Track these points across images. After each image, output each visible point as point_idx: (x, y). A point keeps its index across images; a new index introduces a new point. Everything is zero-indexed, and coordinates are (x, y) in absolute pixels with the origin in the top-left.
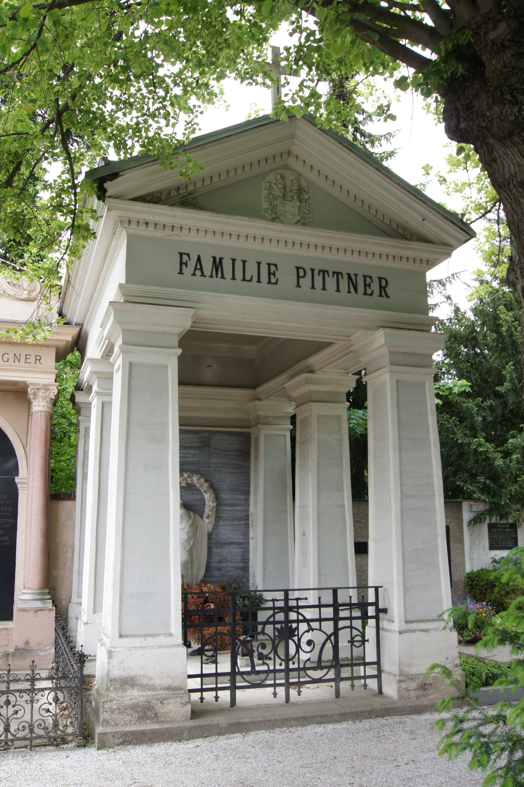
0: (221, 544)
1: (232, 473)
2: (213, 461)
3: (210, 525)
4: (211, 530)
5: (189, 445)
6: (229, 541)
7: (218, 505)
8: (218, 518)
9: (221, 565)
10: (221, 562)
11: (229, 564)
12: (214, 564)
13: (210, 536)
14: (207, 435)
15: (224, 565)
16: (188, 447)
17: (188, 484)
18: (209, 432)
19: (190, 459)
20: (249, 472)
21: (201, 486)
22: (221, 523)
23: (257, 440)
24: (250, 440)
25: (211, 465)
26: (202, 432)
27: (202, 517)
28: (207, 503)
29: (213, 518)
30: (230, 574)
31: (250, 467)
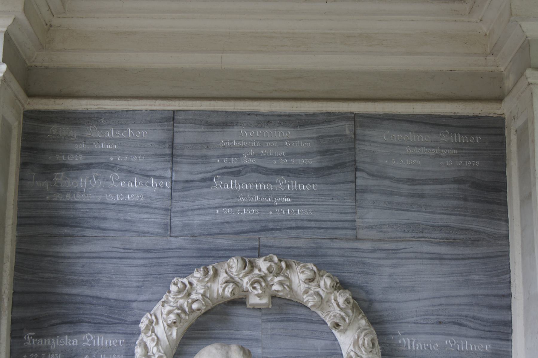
1: (441, 258)
2: (371, 216)
5: (283, 163)
14: (347, 128)
16: (279, 172)
17: (274, 297)
18: (354, 117)
20: (506, 255)
21: (322, 302)
23: (525, 135)
24: (503, 144)
25: (362, 233)
26: (329, 118)
31: (507, 237)
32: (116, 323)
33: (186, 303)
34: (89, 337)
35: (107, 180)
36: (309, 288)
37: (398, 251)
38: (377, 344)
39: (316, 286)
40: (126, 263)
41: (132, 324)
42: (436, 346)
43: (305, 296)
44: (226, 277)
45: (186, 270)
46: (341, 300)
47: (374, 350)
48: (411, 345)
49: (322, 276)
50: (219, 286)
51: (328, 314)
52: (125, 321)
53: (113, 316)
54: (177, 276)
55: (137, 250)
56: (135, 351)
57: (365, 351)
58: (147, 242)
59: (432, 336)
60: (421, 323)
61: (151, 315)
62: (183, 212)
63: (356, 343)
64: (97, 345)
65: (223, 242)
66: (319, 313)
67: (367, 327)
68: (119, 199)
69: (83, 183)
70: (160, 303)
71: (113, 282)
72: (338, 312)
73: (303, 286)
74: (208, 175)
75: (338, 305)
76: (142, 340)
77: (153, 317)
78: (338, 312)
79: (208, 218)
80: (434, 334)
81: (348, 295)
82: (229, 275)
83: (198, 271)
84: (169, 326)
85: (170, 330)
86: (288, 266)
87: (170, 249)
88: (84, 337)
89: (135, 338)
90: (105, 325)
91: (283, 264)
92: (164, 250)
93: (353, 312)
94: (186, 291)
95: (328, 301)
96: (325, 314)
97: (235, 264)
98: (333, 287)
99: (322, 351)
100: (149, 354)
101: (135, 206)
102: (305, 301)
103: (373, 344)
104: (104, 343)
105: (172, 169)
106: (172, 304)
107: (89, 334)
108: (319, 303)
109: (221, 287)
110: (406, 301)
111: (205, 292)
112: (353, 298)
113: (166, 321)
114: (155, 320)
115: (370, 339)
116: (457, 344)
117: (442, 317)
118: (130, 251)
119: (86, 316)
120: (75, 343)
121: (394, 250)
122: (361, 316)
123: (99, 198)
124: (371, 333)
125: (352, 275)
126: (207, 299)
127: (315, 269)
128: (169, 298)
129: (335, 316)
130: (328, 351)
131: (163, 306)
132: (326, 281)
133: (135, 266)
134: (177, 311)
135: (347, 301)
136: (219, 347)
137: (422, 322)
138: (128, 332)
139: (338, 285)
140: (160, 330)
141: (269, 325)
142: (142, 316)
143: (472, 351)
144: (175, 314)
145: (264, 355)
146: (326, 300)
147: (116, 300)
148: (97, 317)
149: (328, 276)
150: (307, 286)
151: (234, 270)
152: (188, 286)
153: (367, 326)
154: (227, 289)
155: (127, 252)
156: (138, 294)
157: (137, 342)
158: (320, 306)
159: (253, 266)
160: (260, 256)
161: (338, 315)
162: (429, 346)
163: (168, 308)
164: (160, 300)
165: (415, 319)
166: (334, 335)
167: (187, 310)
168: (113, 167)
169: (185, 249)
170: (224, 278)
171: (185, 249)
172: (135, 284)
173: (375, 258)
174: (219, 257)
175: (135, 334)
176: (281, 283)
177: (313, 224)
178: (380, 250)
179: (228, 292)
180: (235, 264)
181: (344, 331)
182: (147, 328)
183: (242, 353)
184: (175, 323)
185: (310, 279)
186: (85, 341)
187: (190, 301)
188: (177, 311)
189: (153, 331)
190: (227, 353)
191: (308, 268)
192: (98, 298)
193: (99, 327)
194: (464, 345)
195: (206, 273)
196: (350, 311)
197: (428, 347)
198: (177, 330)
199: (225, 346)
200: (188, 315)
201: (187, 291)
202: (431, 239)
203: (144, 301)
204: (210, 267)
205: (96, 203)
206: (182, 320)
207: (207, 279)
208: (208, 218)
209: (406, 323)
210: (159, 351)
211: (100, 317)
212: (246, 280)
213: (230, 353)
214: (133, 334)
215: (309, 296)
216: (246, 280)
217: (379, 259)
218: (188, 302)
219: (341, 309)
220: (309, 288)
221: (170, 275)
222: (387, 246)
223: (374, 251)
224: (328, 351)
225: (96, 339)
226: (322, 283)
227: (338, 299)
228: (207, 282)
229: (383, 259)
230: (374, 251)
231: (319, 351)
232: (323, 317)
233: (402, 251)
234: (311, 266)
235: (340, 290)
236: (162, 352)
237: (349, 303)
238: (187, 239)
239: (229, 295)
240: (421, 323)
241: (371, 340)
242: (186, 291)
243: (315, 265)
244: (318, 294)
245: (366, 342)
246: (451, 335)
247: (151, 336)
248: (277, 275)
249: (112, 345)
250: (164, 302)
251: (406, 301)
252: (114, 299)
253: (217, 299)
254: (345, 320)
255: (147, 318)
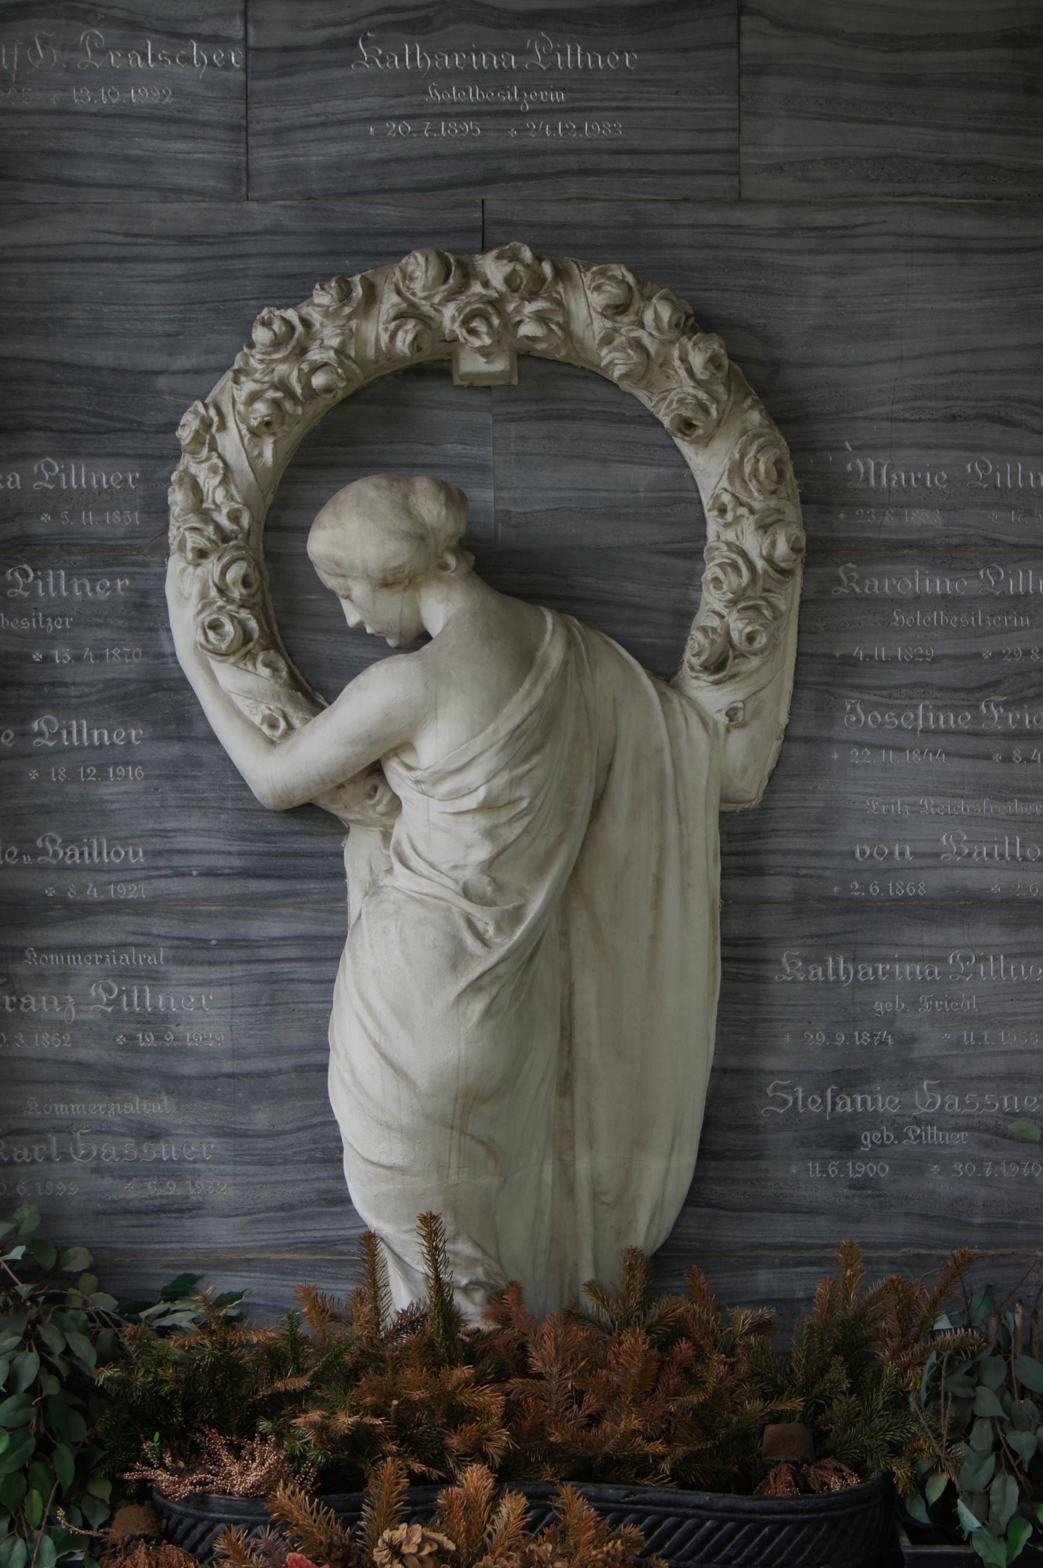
0: (855, 917)
1: (960, 248)
3: (737, 742)
4: (750, 788)
6: (927, 883)
7: (817, 552)
8: (822, 677)
9: (846, 1105)
10: (849, 1079)
11: (926, 1098)
12: (788, 1094)
13: (743, 839)
15: (882, 1101)
17: (524, 356)
19: (554, 132)
21: (649, 367)
22: (857, 716)
27: (664, 668)
28: (713, 527)
29: (771, 683)
30: (939, 1184)
32: (115, 431)
33: (295, 375)
34: (49, 468)
35: (74, 49)
36: (615, 330)
37: (848, 233)
38: (789, 473)
39: (632, 323)
40: (135, 273)
41: (157, 432)
42: (940, 478)
43: (604, 352)
44: (398, 304)
45: (296, 291)
46: (698, 360)
47: (782, 488)
48: (878, 476)
49: (650, 298)
50: (381, 326)
51: (665, 398)
52: (141, 424)
53: (107, 412)
54: (268, 306)
55: (162, 237)
56: (170, 499)
57: (759, 491)
58: (185, 215)
59: (933, 452)
60: (904, 420)
61: (206, 406)
62: (280, 134)
63: (735, 471)
64: (70, 487)
65: (387, 212)
66: (642, 395)
67: (766, 430)
68: (106, 99)
69: (10, 58)
70: (229, 374)
71: (105, 324)
72: (692, 391)
73: (600, 325)
74: (344, 31)
75: (690, 372)
76: (186, 471)
77: (212, 412)
78: (692, 391)
79: (347, 148)
80: (936, 446)
81: (716, 346)
82: (405, 299)
83: (323, 289)
84: (254, 433)
85: (256, 445)
86: (561, 274)
87: (247, 233)
88: (36, 468)
89: (168, 469)
90: (88, 436)
91: (547, 268)
92: (231, 237)
93: (729, 391)
94: (293, 342)
95: (666, 363)
96: (655, 399)
97: (419, 268)
98: (677, 325)
99: (650, 494)
100: (205, 505)
101: (152, 119)
102: (604, 363)
103: (781, 474)
104: (87, 482)
105: (245, 15)
106: (258, 376)
107: (48, 459)
108: (642, 369)
109: (386, 330)
110: (866, 363)
111: (343, 344)
112: (731, 357)
113: (244, 420)
114: (216, 419)
115: (772, 459)
116: (994, 471)
117: (959, 403)
118: (144, 241)
119: (37, 413)
120: (13, 483)
121: (839, 228)
122: (749, 402)
123: (54, 99)
124: (774, 444)
125: (727, 295)
126: (350, 363)
127: (630, 278)
128: (252, 361)
129: (681, 401)
130: (664, 494)
131: (236, 381)
132: (659, 308)
133: (159, 282)
134: (271, 394)
135: (713, 361)
136: (384, 483)
137: (907, 416)
138: (150, 452)
139: (691, 321)
140: (231, 443)
141: (513, 429)
142: (182, 410)
143: (1032, 489)
144: (267, 400)
145: (500, 507)
146: (660, 360)
147: (114, 371)
148: (68, 415)
149: (665, 298)
150: (609, 324)
151: (418, 286)
152: (300, 328)
153: (766, 426)
154: (400, 335)
155: (136, 244)
156: (171, 355)
157: (174, 477)
158: (643, 377)
159: (468, 274)
160: (484, 249)
161: (690, 400)
162: (924, 478)
163: (248, 386)
164: (228, 367)
165: (888, 408)
166: (679, 451)
167: (299, 391)
168: (88, 12)
169: (288, 233)
170: (393, 305)
171: (288, 233)
172: (160, 328)
173: (789, 252)
174: (379, 254)
175: (167, 457)
176: (541, 318)
177: (626, 162)
178: (802, 229)
179: (403, 342)
180: (419, 268)
181: (705, 442)
182: (198, 439)
183: (442, 497)
184: (268, 424)
185: (617, 307)
186: (40, 476)
187: (305, 367)
188: (271, 394)
189: (213, 448)
190: (406, 497)
191: (613, 278)
192: (65, 365)
193: (73, 440)
194: (1014, 474)
195: (345, 294)
196: (721, 389)
197: (921, 482)
198: (275, 443)
199: (398, 480)
200: (303, 404)
201: (298, 340)
202: (937, 199)
203: (185, 372)
204: (357, 278)
205: (46, 113)
206: (287, 418)
207: (347, 310)
208: (347, 148)
209: (866, 419)
210: (230, 497)
211: (73, 416)
212: (449, 310)
213: (412, 498)
214: (161, 457)
215: (616, 349)
216: (449, 310)
217: (800, 252)
218: (300, 370)
219: (699, 384)
220: (615, 330)
221: (252, 303)
222: (821, 218)
223: (786, 232)
224: (664, 494)
225: (67, 471)
226: (649, 317)
227: (691, 358)
228: (349, 317)
229: (811, 252)
230: (786, 232)
231: (642, 495)
232: (649, 405)
233: (860, 230)
234: (619, 271)
235: (695, 334)
236: (239, 500)
237: (718, 367)
238: (293, 207)
239: (406, 351)
240: (904, 420)
241: (775, 464)
242: (295, 343)
243: (630, 270)
244: (637, 345)
245: (762, 468)
246: (981, 449)
247: (208, 459)
248: (532, 296)
249: (110, 487)
250: (238, 372)
251: (866, 363)
252: (108, 369)
253: (376, 362)
254: (707, 412)
255: (196, 413)
